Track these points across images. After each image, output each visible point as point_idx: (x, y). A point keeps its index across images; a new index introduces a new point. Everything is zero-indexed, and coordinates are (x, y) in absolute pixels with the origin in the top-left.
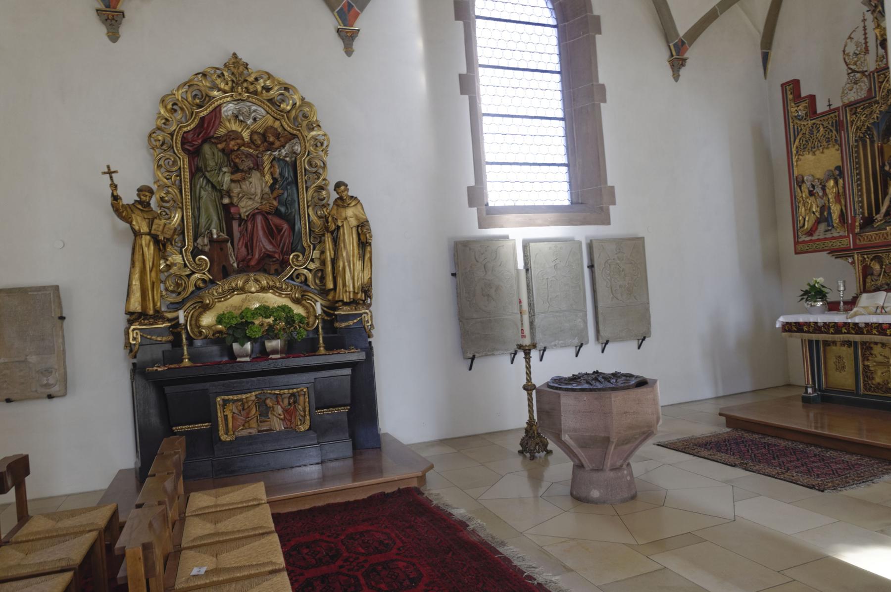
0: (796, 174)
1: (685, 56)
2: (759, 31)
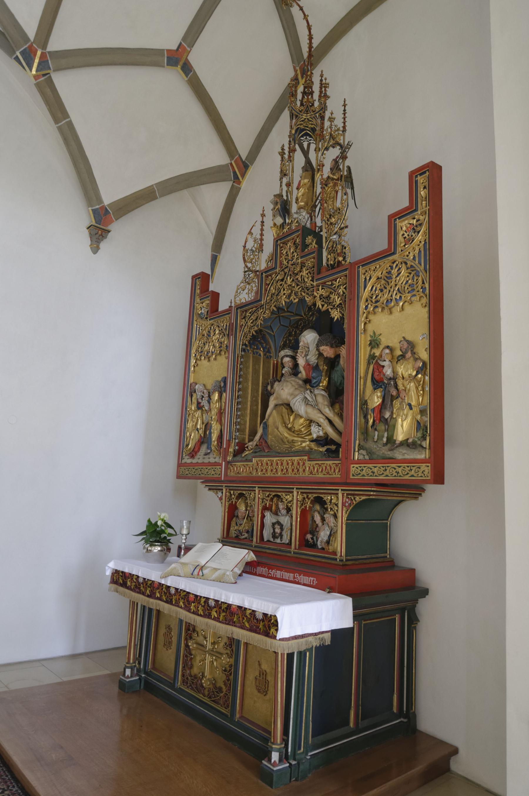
0: (191, 380)
1: (109, 228)
2: (212, 233)
